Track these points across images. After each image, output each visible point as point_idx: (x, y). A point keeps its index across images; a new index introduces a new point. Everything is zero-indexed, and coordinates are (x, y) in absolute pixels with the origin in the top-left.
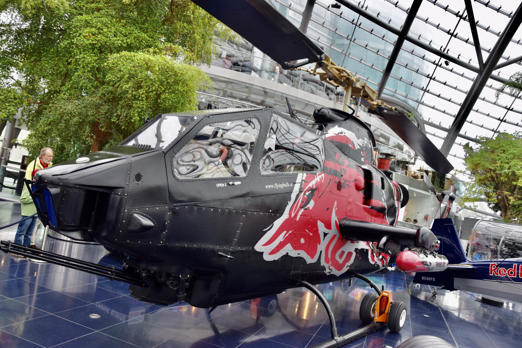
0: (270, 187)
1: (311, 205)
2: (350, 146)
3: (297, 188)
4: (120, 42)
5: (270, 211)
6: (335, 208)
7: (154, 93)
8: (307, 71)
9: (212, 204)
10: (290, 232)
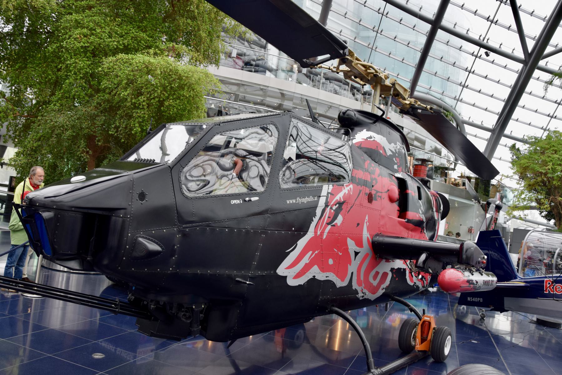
0: (291, 202)
1: (339, 220)
2: (381, 152)
3: (322, 201)
4: (116, 43)
5: (293, 229)
6: (366, 222)
7: (157, 99)
8: (329, 69)
9: (227, 224)
10: (316, 252)
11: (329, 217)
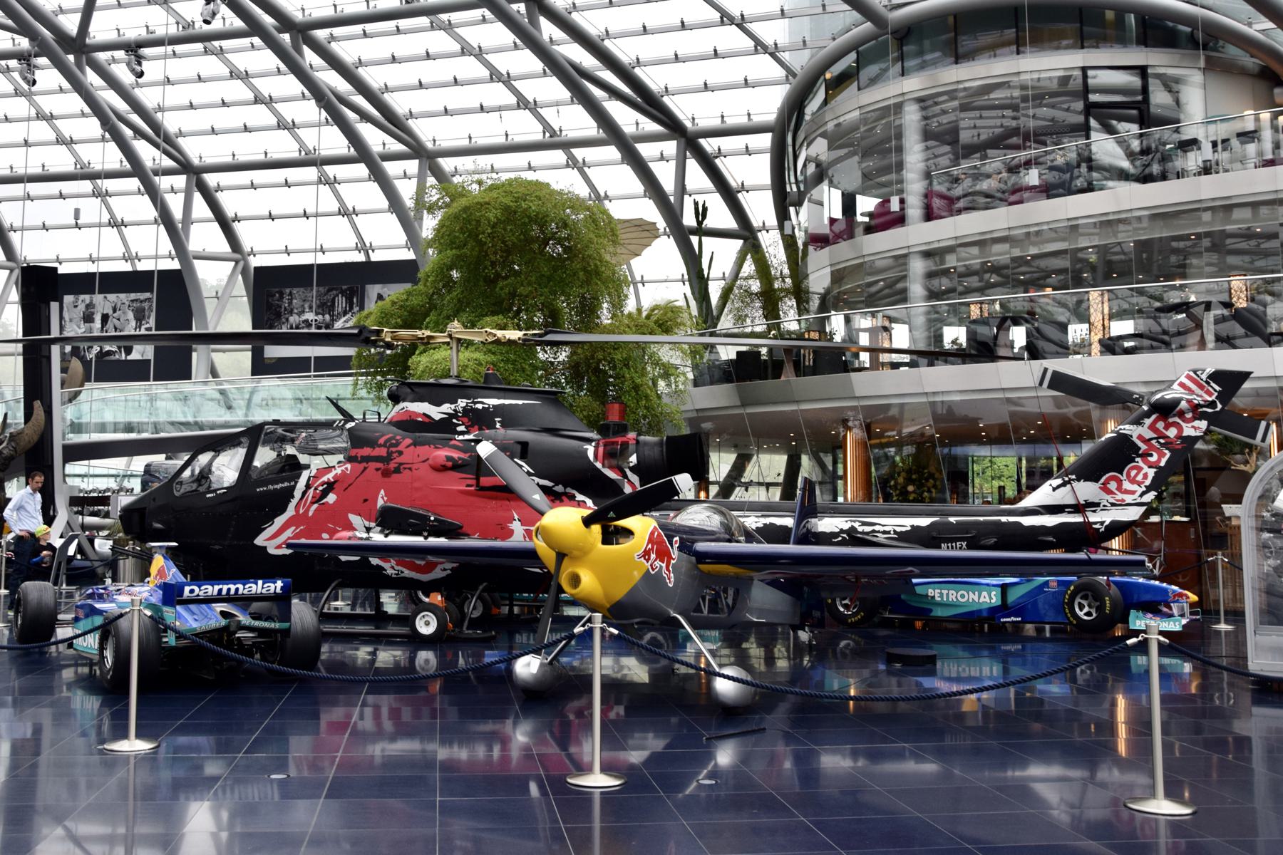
1: (331, 498)
2: (420, 419)
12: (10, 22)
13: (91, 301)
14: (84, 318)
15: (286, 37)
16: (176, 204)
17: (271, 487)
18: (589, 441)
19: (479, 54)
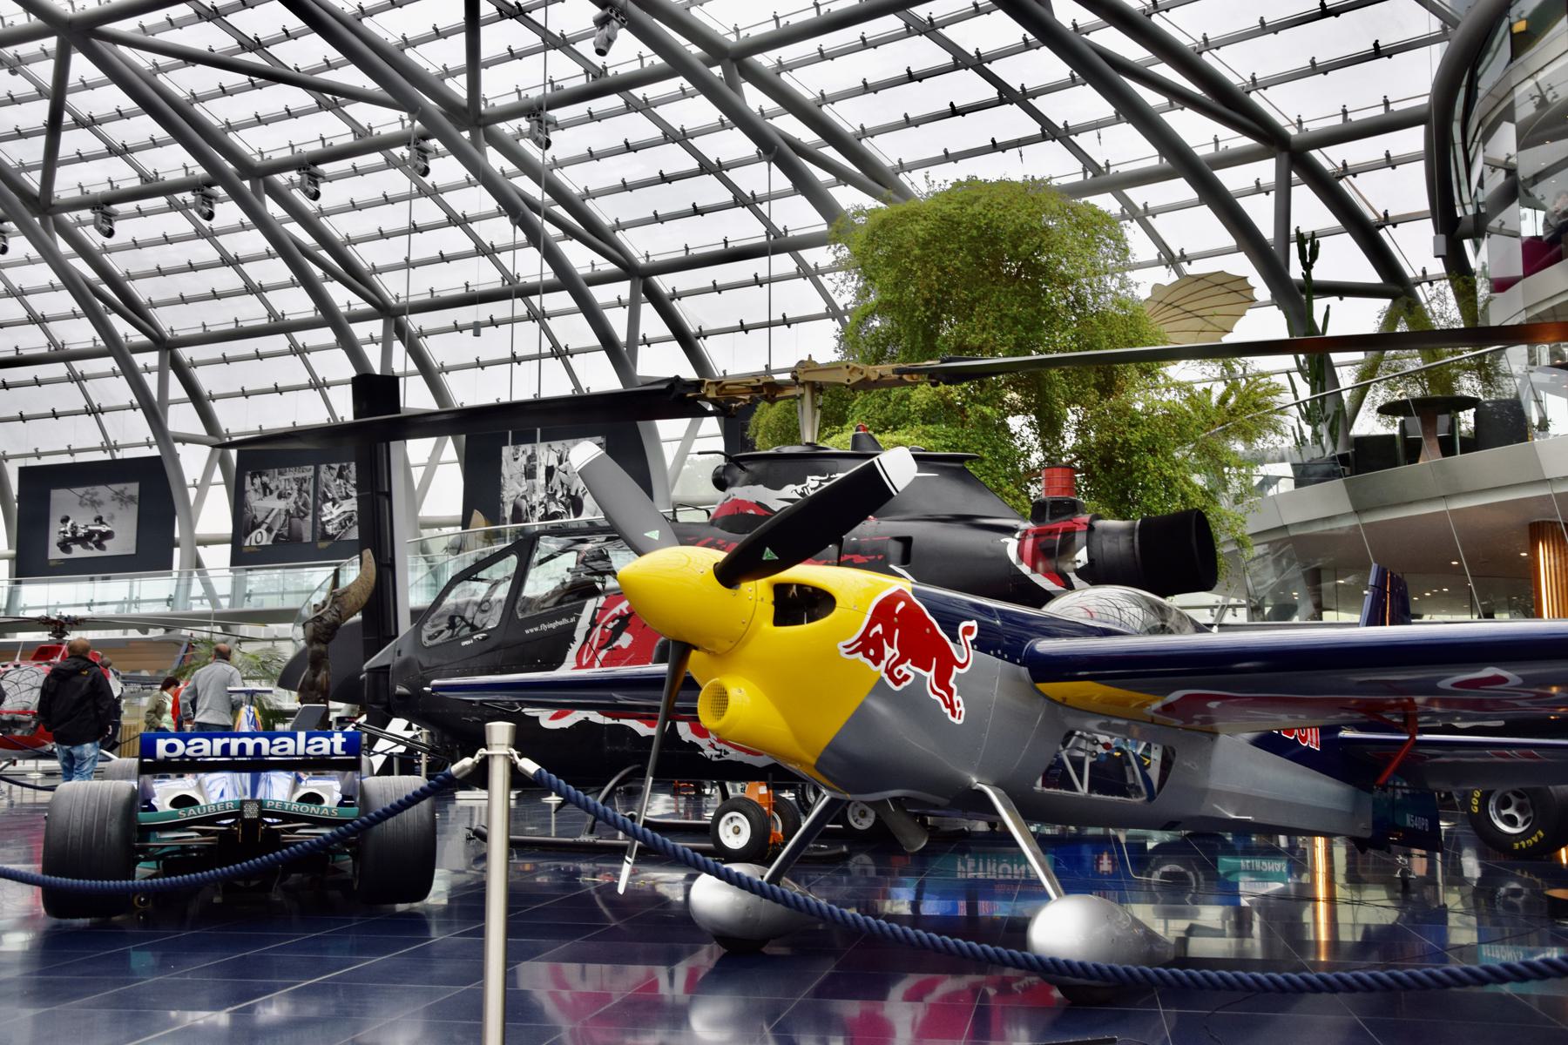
0: (532, 631)
2: (751, 512)
11: (600, 639)
12: (386, 95)
13: (534, 451)
14: (525, 473)
15: (717, 71)
16: (618, 321)
17: (544, 627)
18: (1009, 531)
19: (978, 64)
